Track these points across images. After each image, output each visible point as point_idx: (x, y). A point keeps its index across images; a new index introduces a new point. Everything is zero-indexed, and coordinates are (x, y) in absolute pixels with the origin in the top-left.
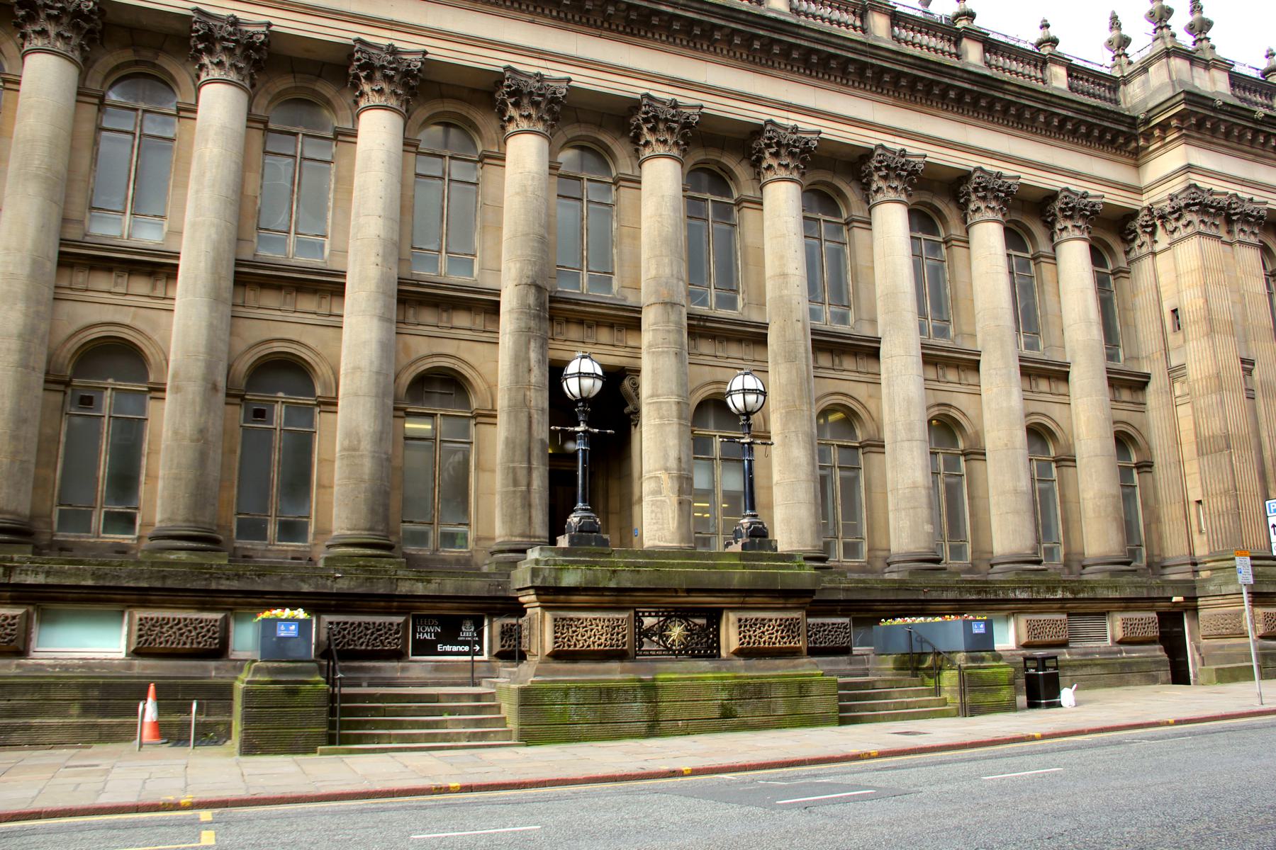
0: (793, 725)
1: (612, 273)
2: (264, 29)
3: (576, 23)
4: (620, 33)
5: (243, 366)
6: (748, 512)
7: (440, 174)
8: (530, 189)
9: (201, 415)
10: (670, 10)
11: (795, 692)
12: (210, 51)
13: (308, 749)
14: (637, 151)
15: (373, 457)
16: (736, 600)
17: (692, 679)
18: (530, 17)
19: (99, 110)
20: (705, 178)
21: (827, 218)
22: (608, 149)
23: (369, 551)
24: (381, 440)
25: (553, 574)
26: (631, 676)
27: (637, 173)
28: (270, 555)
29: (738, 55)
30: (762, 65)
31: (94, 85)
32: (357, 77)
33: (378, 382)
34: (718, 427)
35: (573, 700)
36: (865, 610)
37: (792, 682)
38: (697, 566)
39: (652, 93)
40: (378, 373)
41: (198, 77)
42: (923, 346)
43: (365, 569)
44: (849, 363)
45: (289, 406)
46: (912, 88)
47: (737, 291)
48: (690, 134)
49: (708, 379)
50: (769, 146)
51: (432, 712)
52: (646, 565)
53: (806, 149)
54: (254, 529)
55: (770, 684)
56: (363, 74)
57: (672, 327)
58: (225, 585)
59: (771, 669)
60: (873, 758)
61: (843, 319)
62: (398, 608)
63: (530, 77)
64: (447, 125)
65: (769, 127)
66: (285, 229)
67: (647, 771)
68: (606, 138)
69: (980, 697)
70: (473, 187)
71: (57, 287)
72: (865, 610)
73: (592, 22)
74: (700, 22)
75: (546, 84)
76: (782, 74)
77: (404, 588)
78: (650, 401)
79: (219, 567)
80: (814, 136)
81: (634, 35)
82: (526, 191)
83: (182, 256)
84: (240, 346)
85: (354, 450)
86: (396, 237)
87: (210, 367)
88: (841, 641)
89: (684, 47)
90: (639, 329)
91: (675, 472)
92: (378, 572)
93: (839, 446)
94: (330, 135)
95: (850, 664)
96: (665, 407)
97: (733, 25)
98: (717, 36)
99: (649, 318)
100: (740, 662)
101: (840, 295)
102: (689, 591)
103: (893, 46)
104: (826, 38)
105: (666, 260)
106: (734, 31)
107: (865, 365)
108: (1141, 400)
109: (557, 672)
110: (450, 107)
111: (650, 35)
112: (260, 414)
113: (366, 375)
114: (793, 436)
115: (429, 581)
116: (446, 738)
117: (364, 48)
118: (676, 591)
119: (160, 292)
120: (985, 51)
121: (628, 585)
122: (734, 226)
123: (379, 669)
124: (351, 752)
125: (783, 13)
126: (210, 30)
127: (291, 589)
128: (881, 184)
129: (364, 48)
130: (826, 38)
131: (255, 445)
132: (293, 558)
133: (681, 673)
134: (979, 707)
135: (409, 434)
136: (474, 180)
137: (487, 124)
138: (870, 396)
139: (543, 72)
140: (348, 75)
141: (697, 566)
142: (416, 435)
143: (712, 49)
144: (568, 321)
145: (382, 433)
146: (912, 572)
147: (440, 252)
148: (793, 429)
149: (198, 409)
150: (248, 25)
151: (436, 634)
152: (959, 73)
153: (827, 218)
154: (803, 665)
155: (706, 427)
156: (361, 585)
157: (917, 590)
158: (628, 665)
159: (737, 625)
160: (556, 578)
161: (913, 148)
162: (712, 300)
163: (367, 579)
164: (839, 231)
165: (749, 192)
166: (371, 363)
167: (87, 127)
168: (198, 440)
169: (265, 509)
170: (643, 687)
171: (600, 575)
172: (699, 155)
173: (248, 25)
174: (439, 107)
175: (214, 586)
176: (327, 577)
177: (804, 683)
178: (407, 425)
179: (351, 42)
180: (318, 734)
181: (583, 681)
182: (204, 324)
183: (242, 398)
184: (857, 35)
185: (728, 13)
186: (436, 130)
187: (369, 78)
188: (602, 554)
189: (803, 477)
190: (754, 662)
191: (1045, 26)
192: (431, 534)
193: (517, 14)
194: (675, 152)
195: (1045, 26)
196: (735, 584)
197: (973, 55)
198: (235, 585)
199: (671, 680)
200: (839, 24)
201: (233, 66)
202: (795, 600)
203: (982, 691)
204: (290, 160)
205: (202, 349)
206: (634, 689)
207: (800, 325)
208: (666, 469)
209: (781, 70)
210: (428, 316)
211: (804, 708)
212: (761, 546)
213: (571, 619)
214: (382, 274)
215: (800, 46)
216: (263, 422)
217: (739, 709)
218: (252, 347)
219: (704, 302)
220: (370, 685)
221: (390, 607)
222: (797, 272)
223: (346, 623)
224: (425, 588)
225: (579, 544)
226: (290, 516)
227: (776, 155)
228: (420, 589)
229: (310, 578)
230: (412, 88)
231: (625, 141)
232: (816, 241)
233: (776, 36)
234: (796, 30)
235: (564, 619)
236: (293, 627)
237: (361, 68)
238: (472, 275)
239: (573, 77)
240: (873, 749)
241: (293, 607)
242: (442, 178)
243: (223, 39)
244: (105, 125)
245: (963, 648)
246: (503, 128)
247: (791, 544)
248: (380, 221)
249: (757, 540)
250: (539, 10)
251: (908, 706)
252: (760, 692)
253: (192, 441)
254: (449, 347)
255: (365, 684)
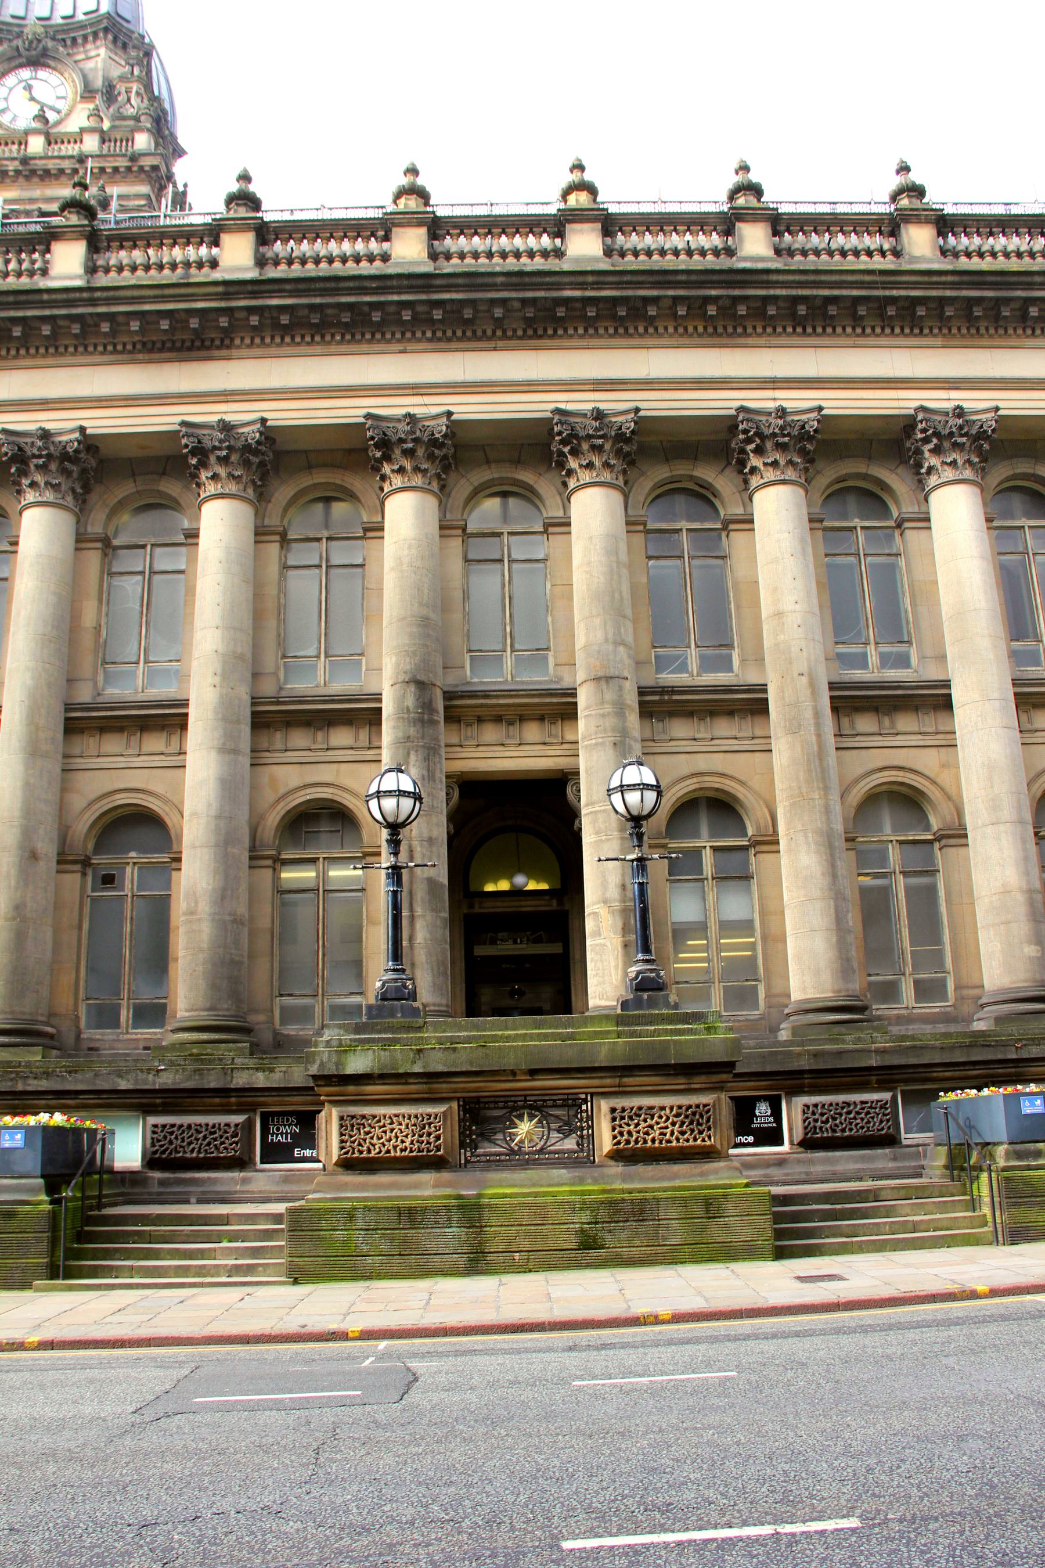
0: (696, 1259)
1: (548, 649)
2: (77, 435)
3: (460, 340)
4: (521, 338)
5: (82, 826)
6: (640, 956)
7: (316, 562)
8: (406, 560)
9: (17, 889)
10: (577, 293)
11: (699, 1210)
12: (387, 458)
13: (24, 1285)
14: (920, 481)
15: (213, 920)
16: (608, 1081)
17: (536, 1195)
18: (400, 347)
19: (105, 555)
20: (1017, 502)
21: (1033, 523)
22: (708, 486)
23: (205, 1036)
24: (223, 898)
25: (334, 1058)
26: (448, 1191)
27: (923, 509)
28: (120, 1045)
29: (691, 329)
30: (730, 336)
31: (273, 520)
32: (561, 454)
33: (217, 828)
34: (713, 835)
35: (360, 1224)
36: (918, 1079)
37: (692, 1198)
38: (545, 1037)
39: (562, 406)
40: (218, 817)
41: (382, 489)
42: (1016, 683)
43: (197, 1058)
44: (905, 722)
45: (143, 867)
46: (971, 320)
47: (730, 646)
48: (986, 446)
49: (686, 771)
50: (926, 440)
51: (208, 1238)
52: (469, 1040)
53: (804, 435)
54: (107, 1017)
55: (658, 1200)
56: (566, 450)
57: (608, 709)
58: (33, 1085)
59: (663, 1178)
60: (663, 1322)
61: (903, 661)
62: (239, 1104)
63: (399, 420)
64: (504, 495)
65: (920, 417)
66: (134, 660)
67: (309, 1329)
68: (526, 476)
69: (1029, 1215)
70: (359, 570)
71: (66, 756)
72: (918, 1079)
73: (479, 333)
74: (625, 300)
75: (789, 418)
76: (762, 341)
77: (241, 1080)
78: (590, 809)
79: (29, 1064)
80: (812, 415)
81: (540, 337)
82: (401, 564)
83: (384, 697)
84: (270, 796)
85: (192, 913)
86: (246, 649)
87: (27, 833)
88: (876, 1126)
89: (611, 336)
90: (577, 718)
91: (617, 905)
92: (210, 1061)
93: (901, 843)
94: (181, 539)
95: (895, 1159)
96: (601, 818)
97: (671, 293)
98: (652, 311)
99: (583, 699)
100: (617, 1169)
101: (894, 626)
102: (533, 1073)
103: (946, 265)
104: (811, 278)
105: (597, 621)
106: (676, 299)
107: (929, 721)
108: (948, 729)
109: (344, 1187)
110: (321, 477)
111: (560, 332)
112: (108, 880)
113: (203, 821)
114: (800, 838)
115: (272, 1070)
116: (201, 1271)
117: (190, 430)
118: (513, 1073)
119: (174, 747)
120: (940, 233)
121: (440, 1068)
122: (723, 558)
123: (214, 1181)
124: (71, 1288)
125: (762, 259)
126: (20, 449)
127: (106, 1086)
128: (934, 461)
129: (190, 430)
130: (811, 278)
131: (102, 918)
132: (145, 1048)
133: (522, 1186)
134: (1027, 1229)
135: (286, 886)
136: (360, 561)
137: (545, 486)
138: (943, 766)
139: (413, 411)
140: (551, 453)
141: (545, 1037)
142: (294, 887)
143: (651, 330)
144: (480, 720)
145: (224, 889)
146: (998, 1020)
147: (318, 657)
148: (800, 827)
149: (13, 883)
150: (60, 434)
151: (294, 1135)
152: (590, 279)
153: (867, 524)
154: (716, 1172)
155: (696, 835)
156: (189, 1079)
157: (1004, 1045)
158: (446, 1176)
159: (609, 1116)
160: (338, 1064)
161: (974, 401)
162: (694, 664)
163: (195, 1071)
164: (890, 538)
165: (737, 510)
166: (209, 805)
167: (273, 569)
168: (14, 919)
169: (117, 994)
170: (460, 1207)
171: (399, 1056)
172: (1000, 472)
173: (60, 434)
174: (306, 481)
175: (20, 1087)
176: (149, 1070)
177: (714, 1197)
178: (332, 873)
179: (549, 415)
180: (37, 1266)
181: (377, 1199)
182: (19, 784)
183: (86, 863)
184: (889, 263)
185: (660, 278)
186: (492, 505)
187: (575, 452)
188: (409, 1029)
189: (817, 893)
190: (640, 1168)
191: (904, 169)
192: (318, 1009)
193: (382, 347)
194: (968, 473)
195: (904, 169)
196: (602, 1059)
197: (920, 243)
198: (43, 1085)
199: (505, 1196)
200: (804, 253)
201: (231, 476)
202: (703, 1078)
203: (1033, 1204)
204: (139, 578)
205: (17, 813)
206: (448, 1209)
207: (804, 680)
208: (605, 901)
209: (759, 335)
210: (299, 738)
211: (714, 1233)
212: (652, 1003)
213: (364, 1117)
214: (221, 696)
215: (776, 298)
216: (114, 889)
217: (608, 1237)
218: (90, 804)
219: (683, 668)
220: (200, 1201)
221: (229, 1104)
222: (798, 607)
223: (173, 1126)
224: (267, 1079)
225: (379, 1015)
226: (147, 995)
227: (937, 451)
228: (260, 1080)
229: (128, 1072)
230: (628, 454)
231: (730, 473)
232: (852, 559)
233: (737, 292)
234: (765, 277)
235: (353, 1117)
236: (19, 1136)
237: (564, 442)
238: (731, 670)
239: (824, 404)
240: (664, 1310)
241: (51, 1110)
242: (501, 561)
243: (215, 448)
244: (290, 563)
245: (1003, 1136)
246: (746, 482)
247: (804, 990)
248: (218, 633)
249: (645, 995)
250: (408, 335)
251: (915, 1227)
252: (642, 1211)
253: (7, 920)
254: (325, 773)
255: (193, 1200)
